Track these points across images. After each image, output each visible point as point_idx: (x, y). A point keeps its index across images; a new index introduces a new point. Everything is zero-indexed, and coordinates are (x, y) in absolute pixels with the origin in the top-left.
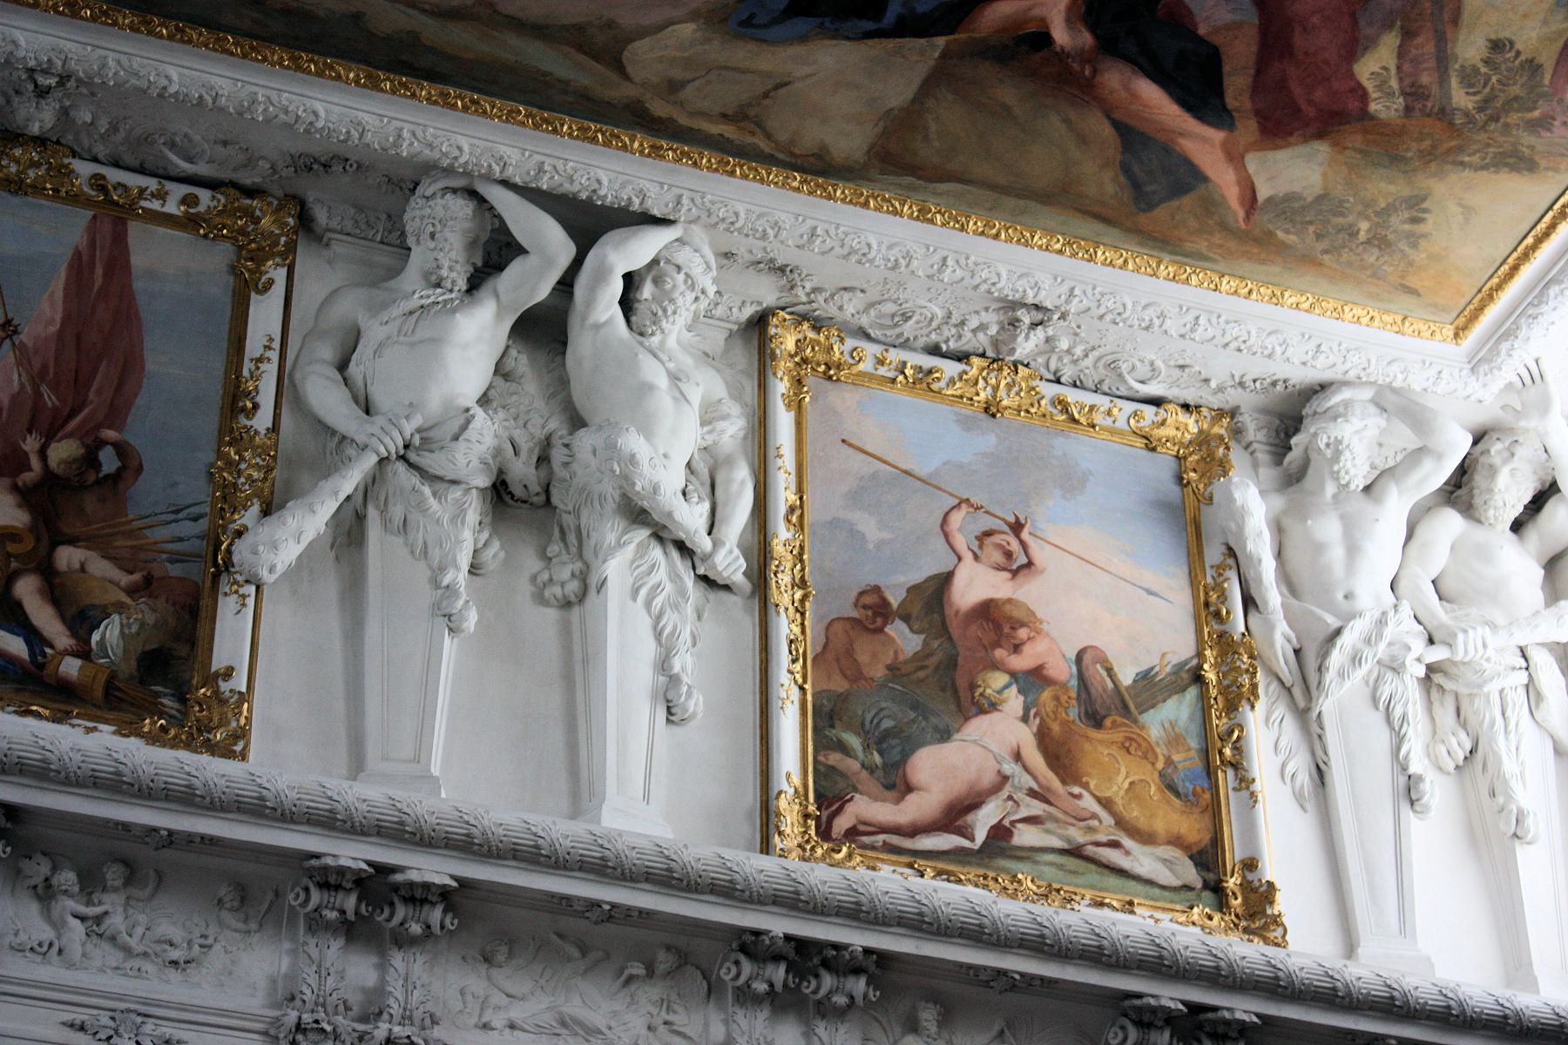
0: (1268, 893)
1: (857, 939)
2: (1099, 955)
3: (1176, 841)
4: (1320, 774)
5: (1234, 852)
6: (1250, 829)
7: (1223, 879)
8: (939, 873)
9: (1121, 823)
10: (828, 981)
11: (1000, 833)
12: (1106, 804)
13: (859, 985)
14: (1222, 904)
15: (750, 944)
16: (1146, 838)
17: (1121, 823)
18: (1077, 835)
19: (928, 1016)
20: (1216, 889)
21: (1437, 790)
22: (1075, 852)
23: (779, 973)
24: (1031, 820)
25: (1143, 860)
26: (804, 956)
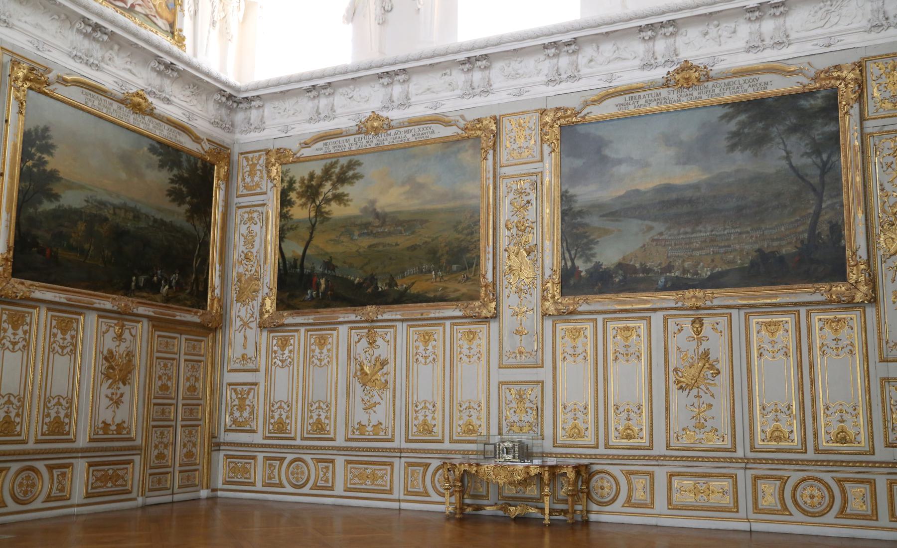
0: (184, 39)
1: (110, 28)
2: (157, 47)
3: (167, 20)
4: (196, 12)
5: (177, 26)
6: (182, 21)
7: (172, 30)
8: (122, 14)
9: (157, 11)
10: (99, 34)
11: (133, 6)
12: (154, 6)
13: (106, 38)
14: (173, 38)
15: (85, 21)
16: (161, 17)
17: (157, 11)
18: (149, 13)
19: (116, 47)
20: (173, 33)
21: (218, 25)
22: (147, 16)
23: (89, 29)
24: (139, 5)
25: (160, 22)
26: (97, 27)
